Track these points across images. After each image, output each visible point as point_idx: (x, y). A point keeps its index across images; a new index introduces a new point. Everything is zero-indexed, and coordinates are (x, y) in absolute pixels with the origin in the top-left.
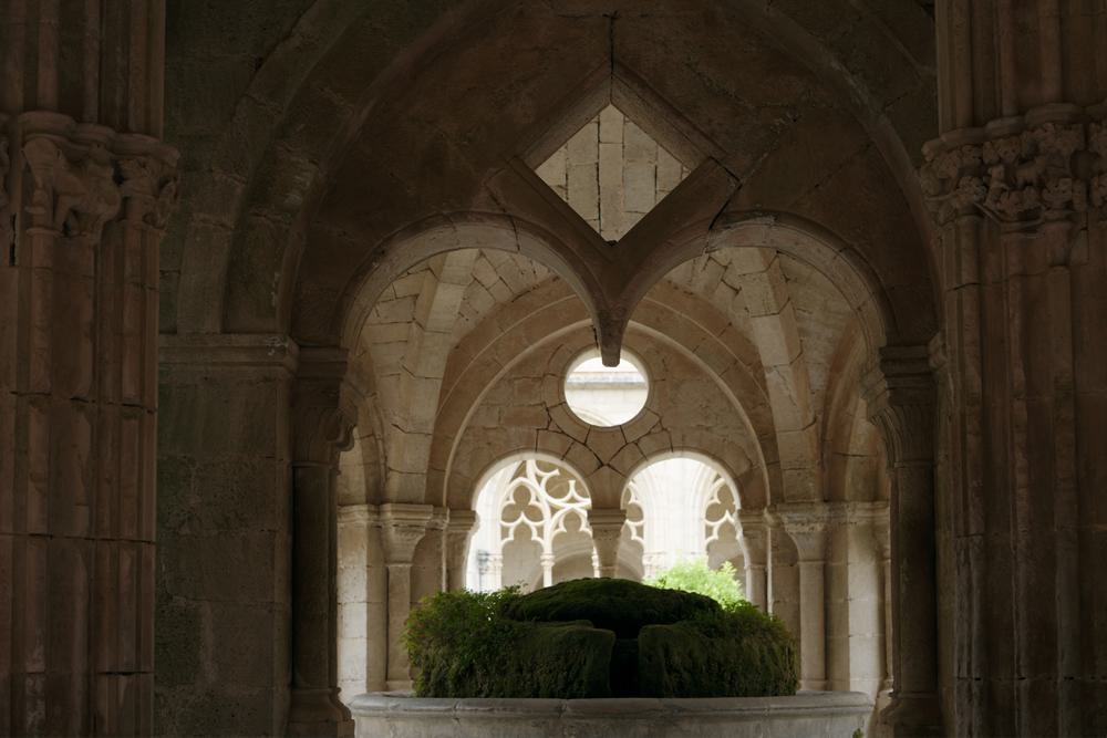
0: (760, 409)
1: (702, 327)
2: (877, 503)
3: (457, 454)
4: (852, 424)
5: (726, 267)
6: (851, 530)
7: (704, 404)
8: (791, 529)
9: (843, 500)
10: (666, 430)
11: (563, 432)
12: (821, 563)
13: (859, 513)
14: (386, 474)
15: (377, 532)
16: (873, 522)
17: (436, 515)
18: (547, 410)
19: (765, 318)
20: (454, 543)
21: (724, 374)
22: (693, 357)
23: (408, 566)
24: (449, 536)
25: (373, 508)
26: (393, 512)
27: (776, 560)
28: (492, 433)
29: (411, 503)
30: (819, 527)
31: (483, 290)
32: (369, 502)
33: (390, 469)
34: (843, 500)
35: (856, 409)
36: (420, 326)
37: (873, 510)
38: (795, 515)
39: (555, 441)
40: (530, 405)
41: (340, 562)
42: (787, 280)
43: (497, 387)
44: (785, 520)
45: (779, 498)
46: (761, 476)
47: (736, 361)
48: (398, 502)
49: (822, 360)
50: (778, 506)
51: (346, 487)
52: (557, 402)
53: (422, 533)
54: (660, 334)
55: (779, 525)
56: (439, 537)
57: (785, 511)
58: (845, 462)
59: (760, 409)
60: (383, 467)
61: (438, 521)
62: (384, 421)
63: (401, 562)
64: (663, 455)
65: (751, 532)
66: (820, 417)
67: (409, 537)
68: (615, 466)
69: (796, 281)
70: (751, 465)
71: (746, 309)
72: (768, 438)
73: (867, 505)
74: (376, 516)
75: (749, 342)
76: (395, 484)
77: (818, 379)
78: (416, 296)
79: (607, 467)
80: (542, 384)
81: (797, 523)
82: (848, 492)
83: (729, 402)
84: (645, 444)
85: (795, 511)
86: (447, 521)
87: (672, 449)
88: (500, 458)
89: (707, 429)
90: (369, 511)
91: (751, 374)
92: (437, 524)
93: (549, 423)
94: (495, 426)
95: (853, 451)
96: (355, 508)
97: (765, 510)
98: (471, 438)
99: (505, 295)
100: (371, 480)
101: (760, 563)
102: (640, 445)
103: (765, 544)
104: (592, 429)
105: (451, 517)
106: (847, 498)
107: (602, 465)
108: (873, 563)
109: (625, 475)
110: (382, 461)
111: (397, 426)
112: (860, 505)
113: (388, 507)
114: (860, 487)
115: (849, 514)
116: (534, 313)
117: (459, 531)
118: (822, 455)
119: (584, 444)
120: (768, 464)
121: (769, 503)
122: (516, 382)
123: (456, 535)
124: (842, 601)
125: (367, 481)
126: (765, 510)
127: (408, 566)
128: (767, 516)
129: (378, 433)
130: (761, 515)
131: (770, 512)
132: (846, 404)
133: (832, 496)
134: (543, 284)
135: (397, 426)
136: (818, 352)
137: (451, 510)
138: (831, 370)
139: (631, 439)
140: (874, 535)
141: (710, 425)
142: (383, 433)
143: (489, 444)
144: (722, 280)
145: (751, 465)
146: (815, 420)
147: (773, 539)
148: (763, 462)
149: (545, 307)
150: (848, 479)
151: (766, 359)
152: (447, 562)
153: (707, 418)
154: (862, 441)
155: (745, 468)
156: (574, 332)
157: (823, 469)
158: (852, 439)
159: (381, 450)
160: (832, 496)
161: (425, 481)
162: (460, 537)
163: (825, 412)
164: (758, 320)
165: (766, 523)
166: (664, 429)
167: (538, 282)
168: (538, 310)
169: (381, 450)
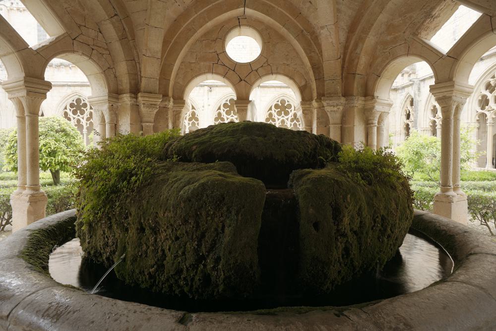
0: (313, 54)
1: (288, 14)
2: (367, 97)
3: (177, 74)
4: (359, 58)
6: (356, 110)
8: (328, 109)
9: (352, 95)
10: (269, 65)
11: (224, 65)
13: (360, 102)
14: (141, 79)
15: (136, 107)
16: (364, 107)
21: (297, 37)
22: (283, 31)
23: (152, 124)
25: (133, 95)
26: (141, 97)
27: (318, 124)
28: (193, 65)
29: (151, 93)
30: (341, 108)
32: (131, 92)
34: (352, 95)
37: (365, 101)
38: (331, 102)
39: (221, 69)
40: (210, 53)
44: (325, 104)
45: (321, 96)
46: (311, 88)
47: (303, 31)
48: (144, 92)
49: (345, 28)
50: (322, 98)
51: (122, 86)
52: (221, 51)
53: (157, 108)
56: (167, 111)
57: (326, 100)
58: (354, 77)
59: (313, 54)
60: (139, 76)
61: (166, 103)
62: (140, 54)
63: (147, 122)
65: (306, 112)
67: (151, 110)
70: (306, 82)
71: (310, 2)
72: (317, 68)
73: (363, 98)
74: (135, 100)
75: (309, 21)
76: (144, 83)
77: (343, 38)
81: (331, 106)
82: (355, 92)
84: (260, 70)
85: (331, 100)
86: (171, 103)
88: (196, 76)
89: (288, 65)
90: (130, 97)
91: (309, 37)
92: (166, 105)
95: (358, 72)
96: (125, 95)
97: (314, 101)
98: (183, 67)
100: (133, 82)
101: (309, 126)
102: (258, 71)
103: (312, 117)
104: (236, 64)
105: (174, 103)
106: (354, 95)
107: (241, 80)
108: (364, 126)
109: (250, 86)
110: (139, 73)
113: (139, 95)
114: (360, 89)
116: (211, 5)
118: (342, 74)
119: (234, 71)
122: (204, 41)
123: (177, 111)
125: (130, 83)
126: (314, 101)
127: (152, 124)
128: (315, 104)
129: (136, 59)
130: (311, 104)
131: (317, 101)
132: (355, 49)
133: (347, 94)
136: (344, 24)
137: (174, 99)
138: (348, 33)
139: (254, 69)
140: (364, 113)
142: (139, 60)
143: (191, 70)
145: (306, 82)
147: (317, 114)
148: (313, 78)
150: (355, 85)
154: (362, 68)
155: (303, 83)
156: (229, 20)
157: (343, 82)
160: (347, 94)
161: (158, 83)
163: (345, 54)
166: (269, 65)
168: (214, 4)
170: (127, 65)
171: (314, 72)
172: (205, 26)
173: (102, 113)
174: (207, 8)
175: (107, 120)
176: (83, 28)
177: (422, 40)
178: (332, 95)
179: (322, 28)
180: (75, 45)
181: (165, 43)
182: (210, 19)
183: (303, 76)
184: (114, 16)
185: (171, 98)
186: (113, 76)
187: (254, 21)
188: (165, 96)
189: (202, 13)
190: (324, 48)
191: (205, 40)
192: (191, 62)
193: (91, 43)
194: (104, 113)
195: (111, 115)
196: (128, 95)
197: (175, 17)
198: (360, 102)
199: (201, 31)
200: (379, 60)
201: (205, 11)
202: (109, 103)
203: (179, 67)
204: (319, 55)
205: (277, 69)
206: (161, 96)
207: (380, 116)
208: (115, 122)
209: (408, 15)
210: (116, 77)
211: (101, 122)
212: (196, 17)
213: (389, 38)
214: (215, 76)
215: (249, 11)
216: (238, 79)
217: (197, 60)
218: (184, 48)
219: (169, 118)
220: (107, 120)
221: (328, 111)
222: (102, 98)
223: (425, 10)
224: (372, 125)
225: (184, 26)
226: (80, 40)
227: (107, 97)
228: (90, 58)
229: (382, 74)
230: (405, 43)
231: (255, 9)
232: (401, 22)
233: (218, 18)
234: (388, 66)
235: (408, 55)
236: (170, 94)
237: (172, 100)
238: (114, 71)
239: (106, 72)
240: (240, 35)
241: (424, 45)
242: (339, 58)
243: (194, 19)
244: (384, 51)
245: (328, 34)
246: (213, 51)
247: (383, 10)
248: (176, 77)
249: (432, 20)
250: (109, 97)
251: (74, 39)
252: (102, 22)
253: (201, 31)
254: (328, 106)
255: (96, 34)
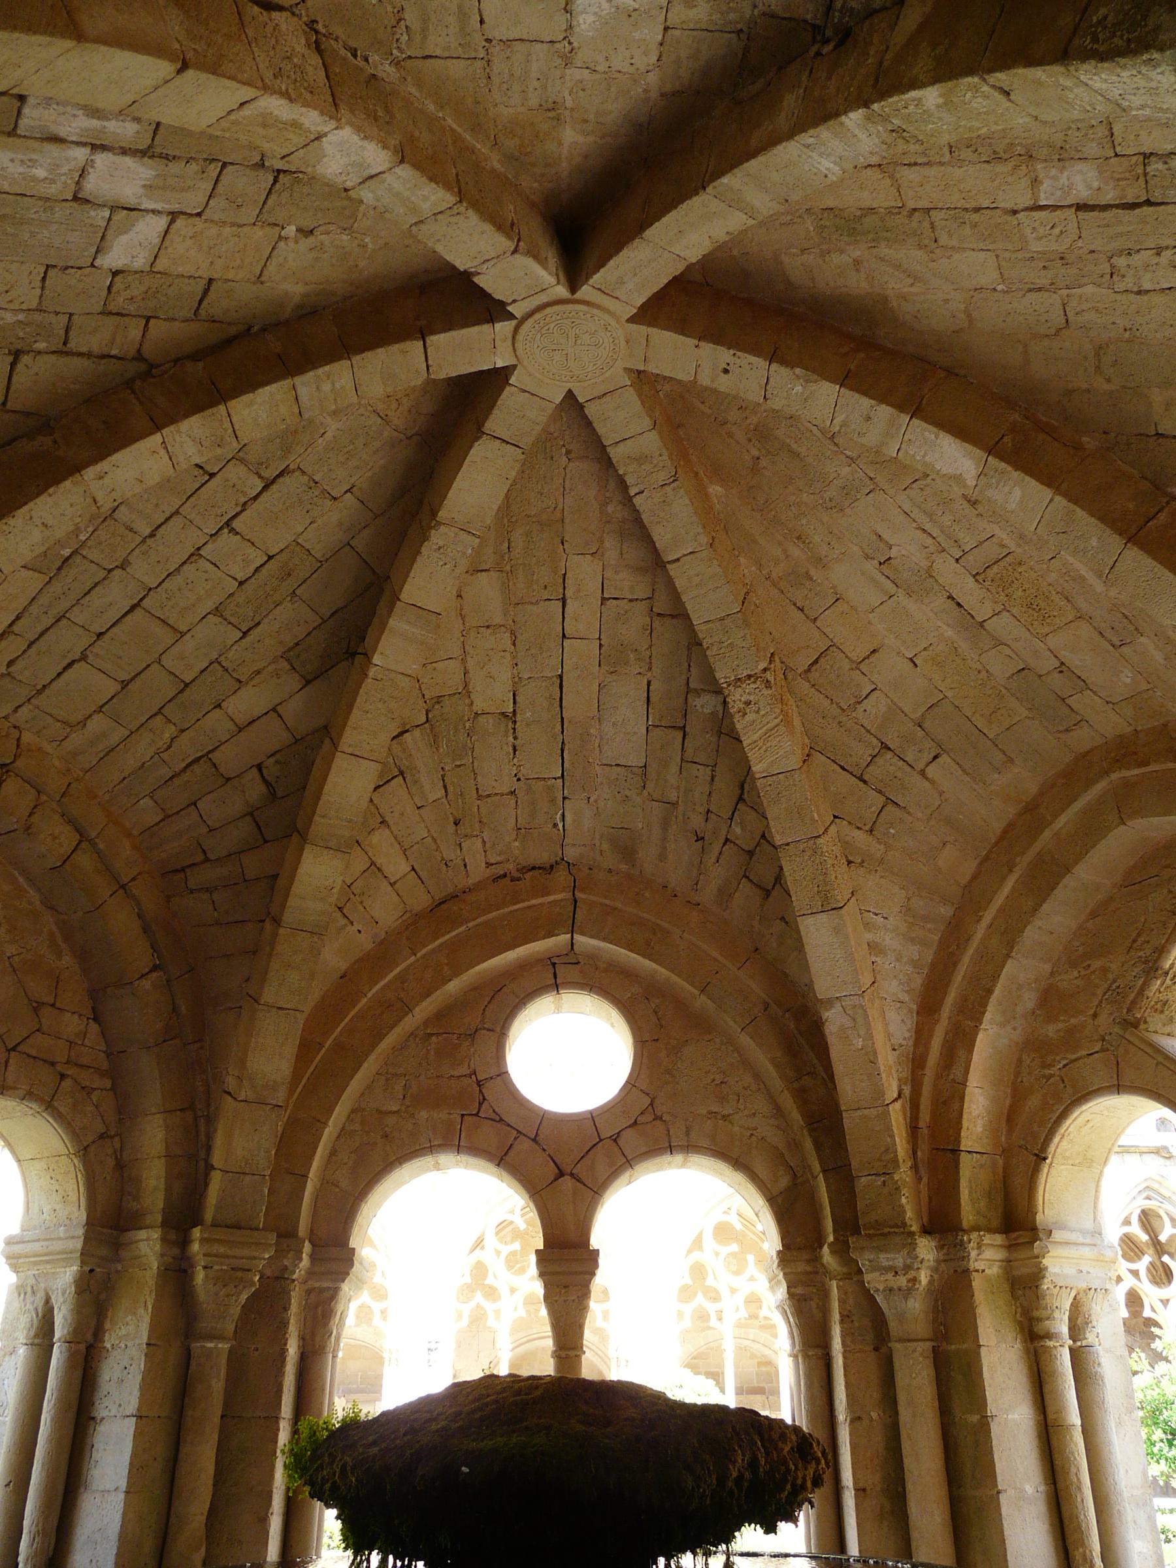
1: (715, 954)
3: (333, 1153)
5: (751, 853)
6: (977, 1283)
7: (719, 1078)
8: (874, 1280)
10: (658, 1118)
11: (501, 1120)
12: (928, 1345)
13: (989, 1254)
14: (207, 1175)
17: (280, 1253)
18: (479, 1083)
19: (824, 916)
20: (316, 1307)
24: (309, 1292)
25: (172, 1236)
27: (848, 1340)
28: (390, 1121)
31: (385, 885)
33: (213, 1168)
35: (967, 1071)
36: (275, 920)
41: (106, 1338)
42: (849, 862)
43: (400, 1048)
44: (864, 1260)
49: (906, 997)
51: (137, 1198)
54: (654, 965)
55: (854, 1273)
64: (658, 1160)
66: (907, 1091)
68: (583, 1176)
69: (861, 864)
71: (783, 919)
73: (999, 1239)
75: (786, 975)
78: (275, 877)
79: (567, 1178)
80: (472, 1044)
82: (968, 1213)
83: (757, 1076)
84: (630, 1140)
86: (305, 1262)
87: (671, 1149)
89: (725, 1118)
90: (164, 1240)
92: (286, 1268)
93: (480, 1104)
94: (395, 1109)
96: (143, 1234)
99: (421, 900)
106: (965, 1225)
107: (561, 1174)
108: (1018, 1345)
110: (203, 1154)
111: (229, 1093)
112: (988, 1239)
113: (196, 1232)
115: (973, 1254)
117: (325, 1284)
118: (914, 1153)
119: (534, 1140)
120: (824, 1171)
121: (831, 1238)
124: (975, 1418)
125: (168, 1190)
127: (224, 1346)
134: (479, 886)
135: (229, 1093)
141: (726, 1112)
142: (209, 1105)
144: (745, 876)
146: (899, 1096)
147: (842, 1302)
148: (817, 1167)
149: (479, 920)
151: (823, 987)
152: (302, 1338)
153: (722, 1099)
154: (980, 1129)
155: (784, 1182)
156: (523, 968)
157: (920, 1179)
158: (965, 1123)
159: (203, 1137)
162: (326, 1295)
164: (810, 920)
165: (826, 1272)
166: (658, 1118)
167: (471, 881)
168: (471, 924)
169: (203, 1137)
170: (167, 1127)
171: (818, 1146)
172: (438, 993)
173: (48, 1301)
174: (447, 937)
175: (60, 1330)
176: (46, 1011)
177: (1152, 1045)
178: (886, 1230)
179: (830, 1003)
180: (11, 1068)
181: (306, 1050)
182: (457, 974)
183: (782, 1154)
184: (150, 972)
185: (307, 1243)
186: (111, 1162)
187: (606, 970)
188: (287, 1235)
189: (433, 951)
190: (838, 1069)
191: (438, 1034)
192: (384, 1109)
193: (60, 1057)
194: (53, 1300)
195: (79, 1309)
196: (156, 1234)
197: (344, 966)
198: (989, 1254)
199: (423, 1010)
200: (1033, 1102)
201: (441, 945)
202: (83, 1263)
203: (343, 1129)
204: (830, 1085)
205: (687, 1133)
206: (272, 1238)
207: (1076, 1306)
208: (89, 1337)
209: (1097, 964)
210: (120, 1166)
211: (36, 1336)
212: (411, 965)
213: (1051, 1030)
214: (464, 1158)
215: (584, 942)
216: (552, 1169)
217: (407, 1102)
218: (365, 1065)
219: (292, 1321)
220: (60, 1330)
221: (878, 1290)
222: (57, 1246)
223: (1141, 953)
224: (1051, 1343)
225: (370, 995)
226: (33, 1052)
227: (79, 1245)
228: (49, 1105)
229: (1052, 1148)
230: (1103, 1050)
231: (604, 940)
232: (1078, 982)
233: (478, 968)
234: (1068, 1122)
235: (1119, 1088)
236: (303, 1230)
237: (307, 1248)
238: (118, 1146)
239: (92, 1148)
240: (558, 1010)
241: (1160, 1059)
242: (896, 1100)
243: (406, 969)
244: (1047, 1072)
245: (848, 1023)
246: (463, 1070)
247: (1012, 947)
248: (329, 1161)
249: (1168, 982)
250: (87, 1240)
251: (14, 1049)
252: (109, 990)
253: (423, 1010)
254: (873, 1269)
255: (82, 1027)
